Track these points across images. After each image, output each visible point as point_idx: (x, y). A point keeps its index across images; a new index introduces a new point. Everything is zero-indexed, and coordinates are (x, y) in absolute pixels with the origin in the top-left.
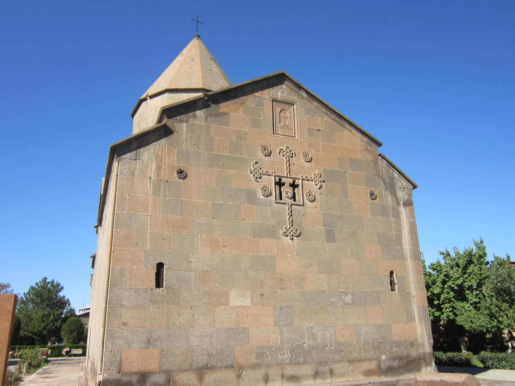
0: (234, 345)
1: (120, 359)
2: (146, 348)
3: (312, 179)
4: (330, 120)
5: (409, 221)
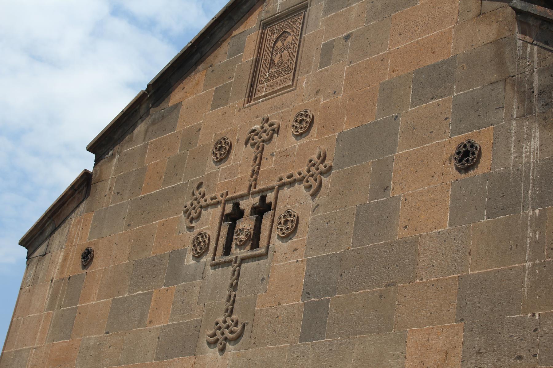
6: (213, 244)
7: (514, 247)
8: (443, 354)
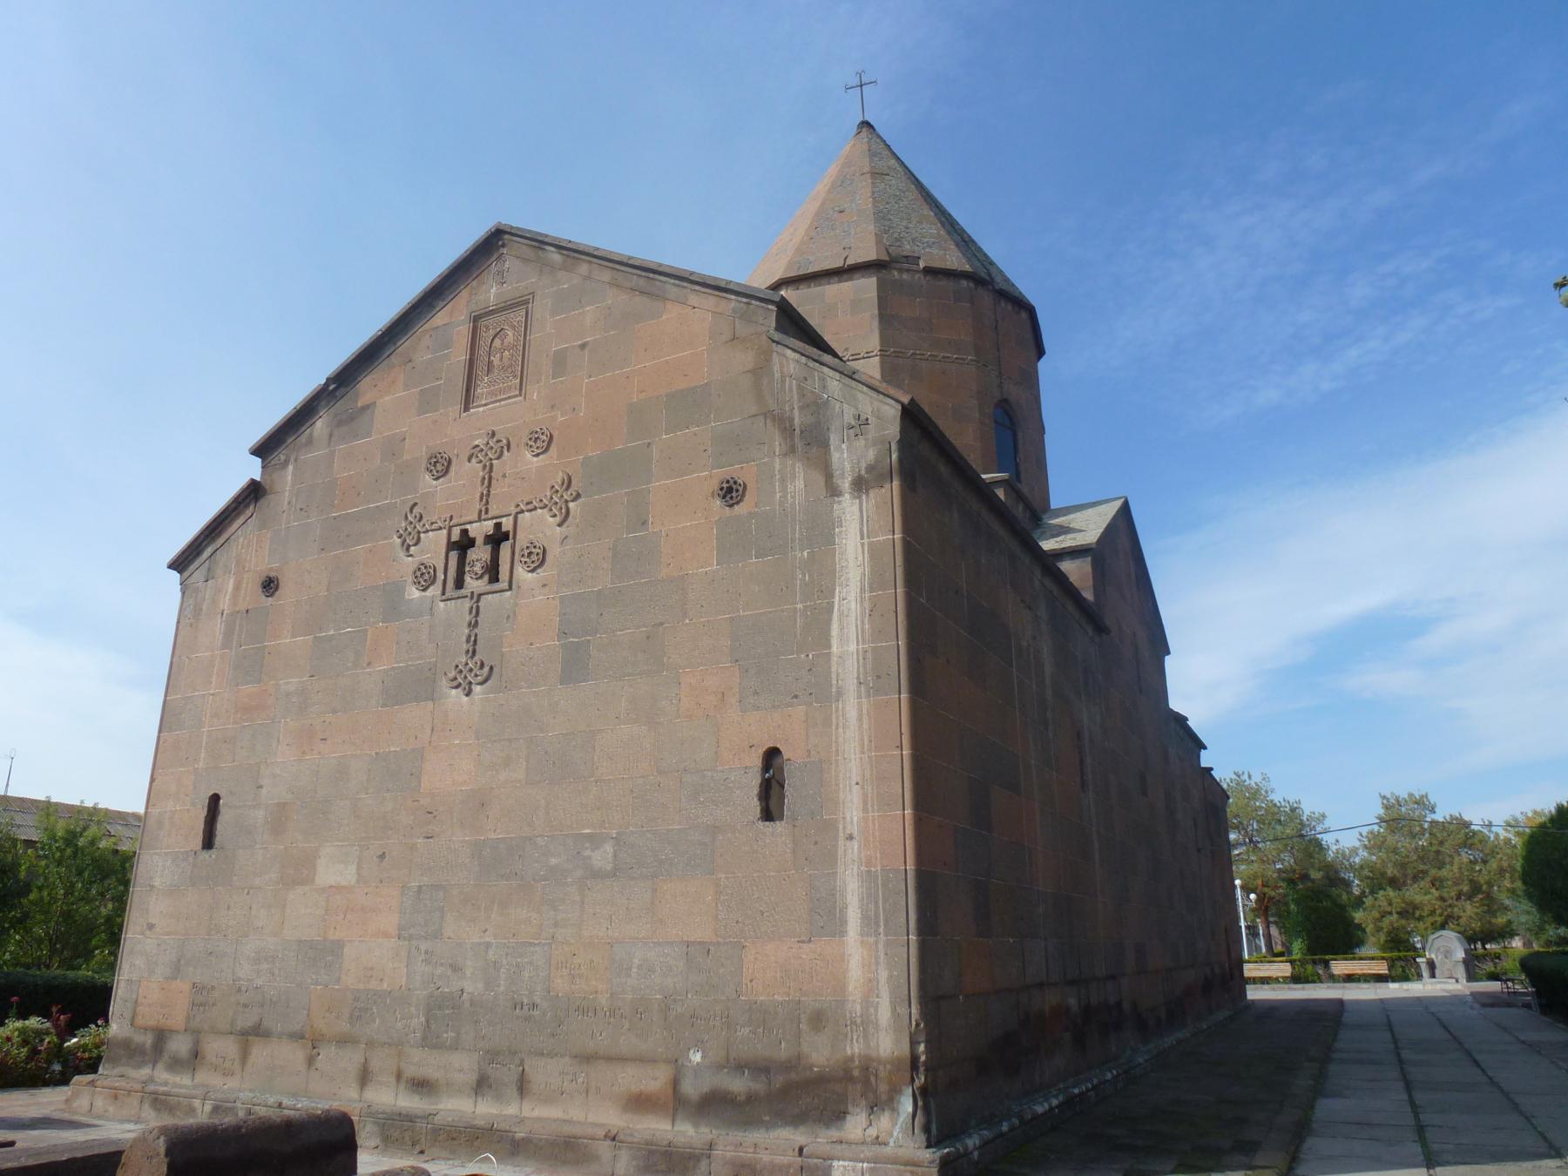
0: (312, 984)
6: (441, 576)
7: (784, 588)
8: (720, 696)
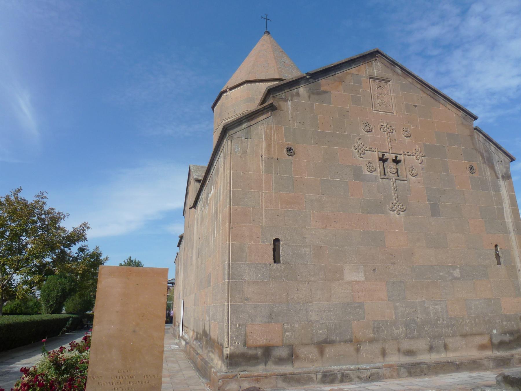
0: (352, 320)
1: (245, 332)
2: (268, 322)
3: (413, 154)
4: (425, 96)
5: (509, 194)
